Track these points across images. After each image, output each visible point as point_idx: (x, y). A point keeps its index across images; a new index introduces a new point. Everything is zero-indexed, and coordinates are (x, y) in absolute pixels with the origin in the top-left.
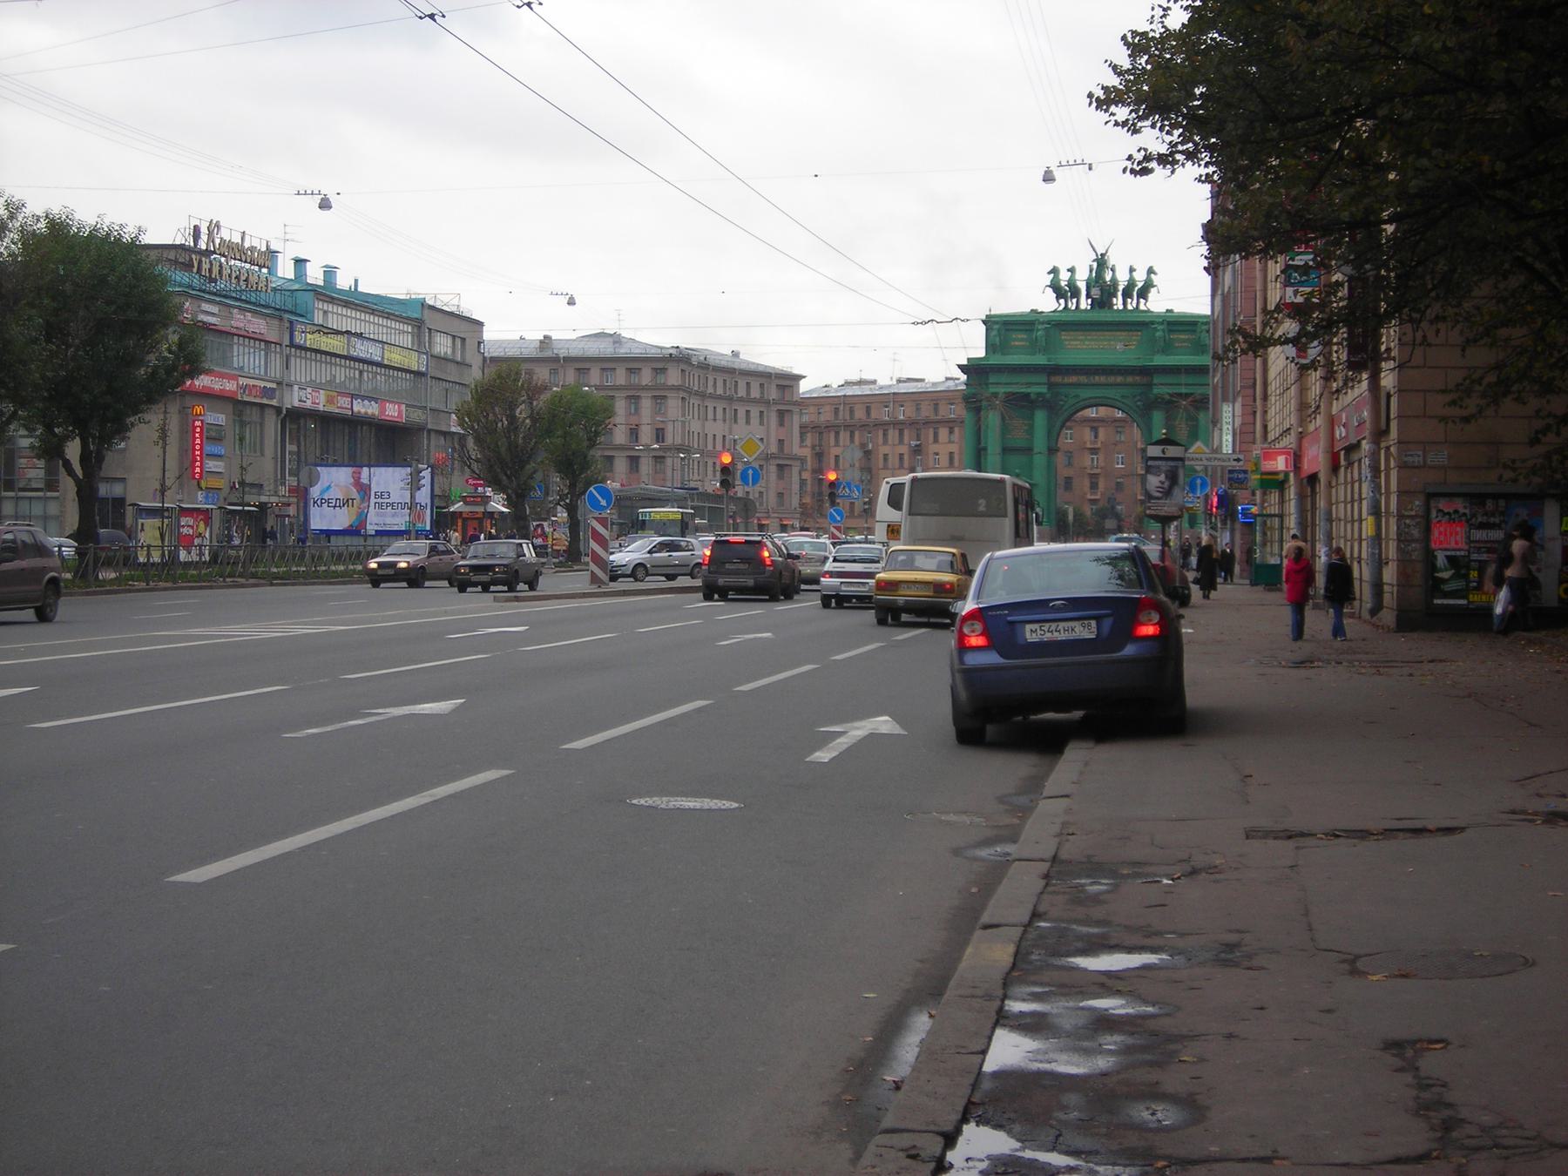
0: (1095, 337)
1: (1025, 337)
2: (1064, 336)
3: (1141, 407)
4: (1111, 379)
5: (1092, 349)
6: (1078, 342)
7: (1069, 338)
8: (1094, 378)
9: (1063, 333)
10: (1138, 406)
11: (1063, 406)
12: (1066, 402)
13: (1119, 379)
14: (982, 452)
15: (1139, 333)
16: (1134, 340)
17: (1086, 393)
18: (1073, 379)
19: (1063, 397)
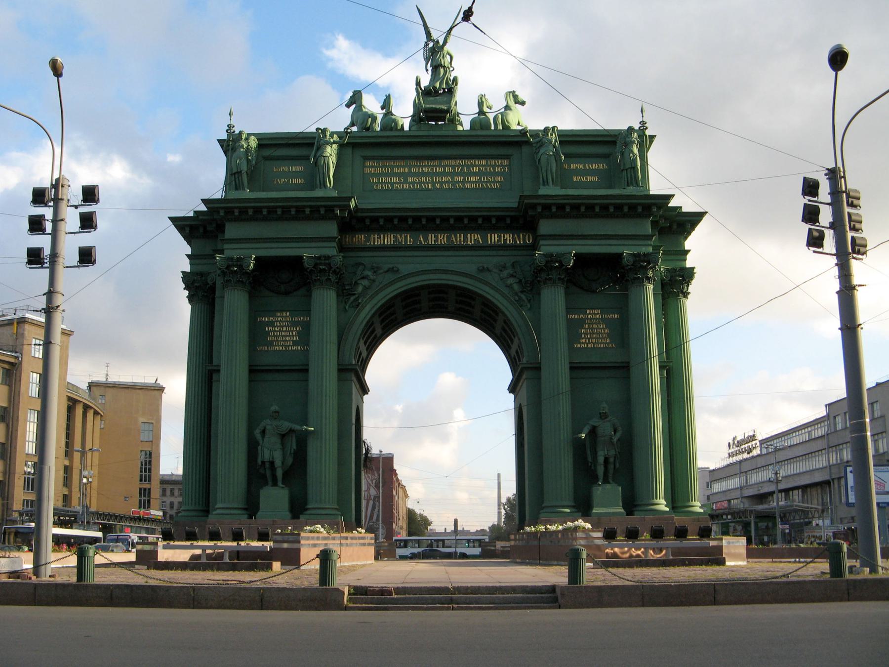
0: (426, 170)
1: (299, 168)
2: (371, 167)
3: (516, 287)
4: (459, 238)
5: (421, 190)
6: (395, 179)
7: (379, 170)
8: (426, 239)
9: (367, 164)
10: (510, 287)
11: (366, 288)
12: (374, 281)
13: (473, 238)
14: (215, 376)
15: (506, 162)
16: (498, 174)
17: (408, 265)
18: (388, 239)
19: (369, 273)
